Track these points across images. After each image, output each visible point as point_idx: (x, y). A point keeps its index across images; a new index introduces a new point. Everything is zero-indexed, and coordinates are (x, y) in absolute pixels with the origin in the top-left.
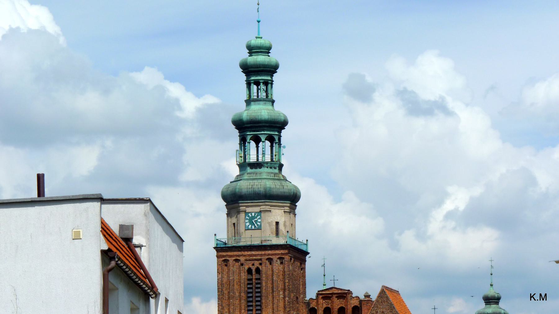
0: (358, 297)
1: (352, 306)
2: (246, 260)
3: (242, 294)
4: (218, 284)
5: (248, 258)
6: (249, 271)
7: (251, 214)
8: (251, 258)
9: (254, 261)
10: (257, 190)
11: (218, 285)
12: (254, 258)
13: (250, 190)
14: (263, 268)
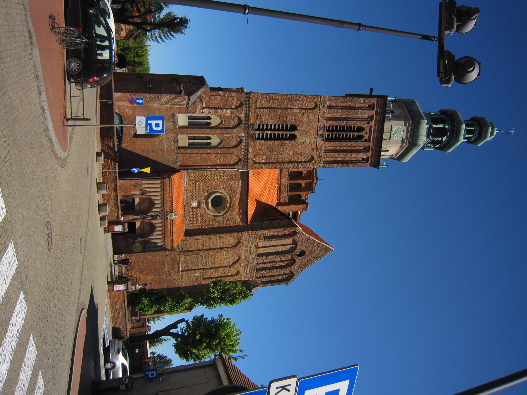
0: (307, 199)
1: (302, 195)
2: (371, 127)
3: (345, 122)
6: (361, 129)
7: (402, 131)
10: (421, 138)
12: (372, 135)
13: (421, 133)
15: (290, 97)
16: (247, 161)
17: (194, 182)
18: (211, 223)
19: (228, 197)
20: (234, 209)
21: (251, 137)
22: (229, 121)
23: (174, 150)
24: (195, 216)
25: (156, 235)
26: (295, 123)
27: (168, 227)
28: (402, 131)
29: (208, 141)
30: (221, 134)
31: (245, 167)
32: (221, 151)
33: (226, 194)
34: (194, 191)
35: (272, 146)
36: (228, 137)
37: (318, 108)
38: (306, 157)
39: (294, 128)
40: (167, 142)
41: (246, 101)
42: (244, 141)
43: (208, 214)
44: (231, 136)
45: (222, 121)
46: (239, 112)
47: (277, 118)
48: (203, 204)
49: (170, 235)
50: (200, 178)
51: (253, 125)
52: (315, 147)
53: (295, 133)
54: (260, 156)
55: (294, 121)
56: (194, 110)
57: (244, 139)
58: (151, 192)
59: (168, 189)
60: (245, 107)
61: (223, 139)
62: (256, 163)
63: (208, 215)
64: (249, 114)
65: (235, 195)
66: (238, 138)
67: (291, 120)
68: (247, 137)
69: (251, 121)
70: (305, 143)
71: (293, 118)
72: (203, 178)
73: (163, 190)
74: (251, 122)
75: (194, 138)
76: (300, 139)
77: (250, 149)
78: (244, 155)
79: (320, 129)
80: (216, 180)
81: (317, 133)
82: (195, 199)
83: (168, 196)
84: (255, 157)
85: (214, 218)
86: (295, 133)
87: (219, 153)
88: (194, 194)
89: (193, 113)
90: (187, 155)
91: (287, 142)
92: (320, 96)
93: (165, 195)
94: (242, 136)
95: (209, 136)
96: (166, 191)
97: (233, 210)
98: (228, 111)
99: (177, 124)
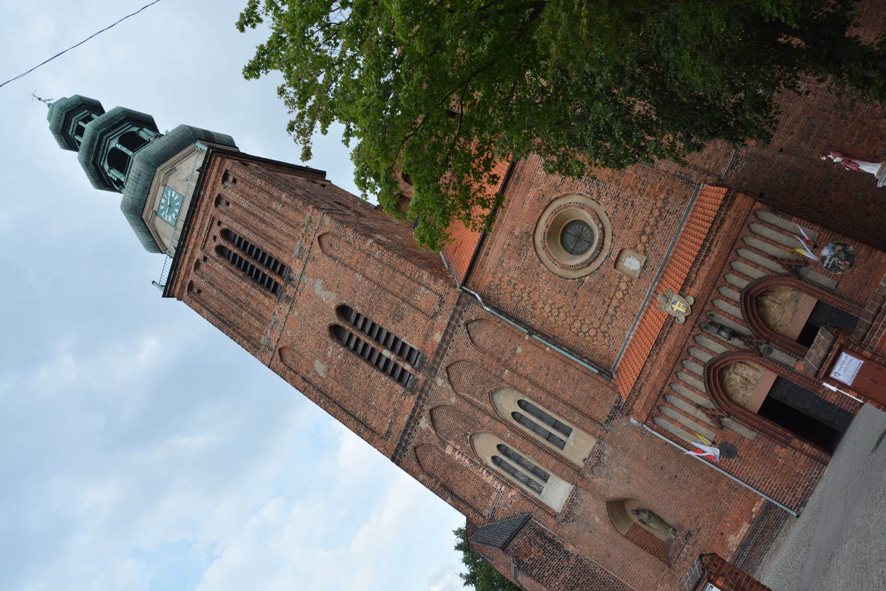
3: (243, 287)
4: (213, 324)
5: (200, 243)
8: (203, 235)
9: (211, 234)
11: (215, 325)
12: (205, 229)
14: (228, 222)
15: (322, 401)
16: (455, 310)
17: (604, 328)
18: (613, 188)
19: (539, 237)
20: (538, 200)
21: (425, 365)
22: (458, 429)
23: (610, 442)
24: (648, 230)
25: (756, 265)
26: (329, 340)
27: (707, 278)
28: (163, 204)
29: (521, 411)
30: (485, 412)
31: (463, 300)
32: (502, 372)
33: (542, 253)
34: (615, 303)
35: (390, 316)
36: (473, 394)
37: (280, 346)
38: (334, 250)
39: (335, 331)
40: (615, 470)
41: (405, 450)
42: (443, 365)
43: (610, 219)
44: (468, 393)
45: (471, 441)
46: (428, 436)
47: (359, 375)
48: (609, 256)
49: (713, 248)
50: (585, 329)
51: (413, 393)
52: (310, 266)
53: (336, 320)
54: (423, 307)
55: (331, 347)
56: (519, 502)
57: (441, 371)
58: (698, 406)
59: (646, 390)
60: (412, 437)
61: (486, 396)
62: (441, 296)
63: (610, 216)
64: (411, 417)
65: (521, 238)
66: (452, 378)
67: (335, 351)
68: (433, 371)
69: (411, 401)
70: (327, 287)
71: (329, 353)
72: (577, 325)
73: (663, 395)
74: (411, 400)
75: (549, 437)
76: (331, 300)
77: (438, 337)
78: (456, 333)
79: (288, 299)
80: (550, 301)
81: (296, 293)
82: (625, 278)
83: (658, 371)
84: (436, 314)
85: (599, 197)
86: (336, 320)
87: (507, 371)
88: (619, 295)
89: (524, 494)
90: (585, 410)
91: (357, 307)
92: (269, 367)
93: (664, 377)
94: (443, 381)
95: (515, 423)
96: (654, 387)
97: (543, 195)
98: (449, 451)
99: (569, 496)
